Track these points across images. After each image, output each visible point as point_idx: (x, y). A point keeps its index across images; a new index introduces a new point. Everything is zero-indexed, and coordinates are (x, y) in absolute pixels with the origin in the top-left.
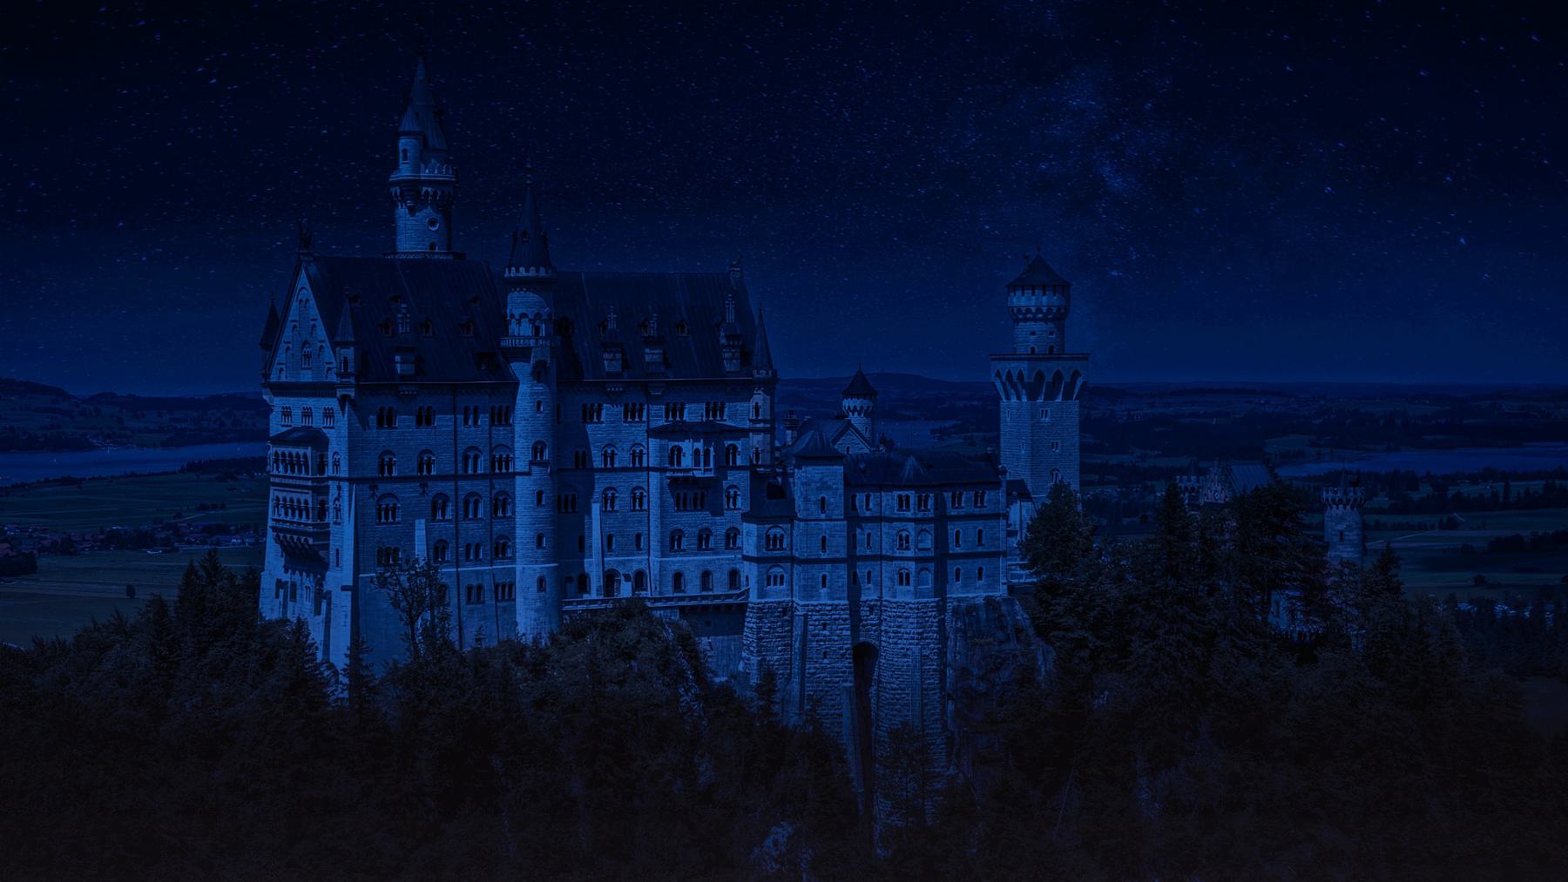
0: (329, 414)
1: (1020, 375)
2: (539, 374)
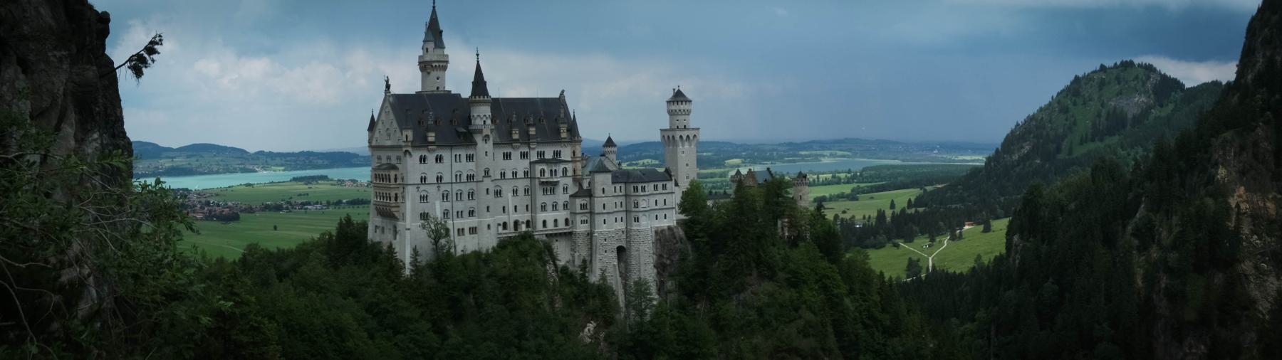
0: (399, 158)
2: (486, 138)
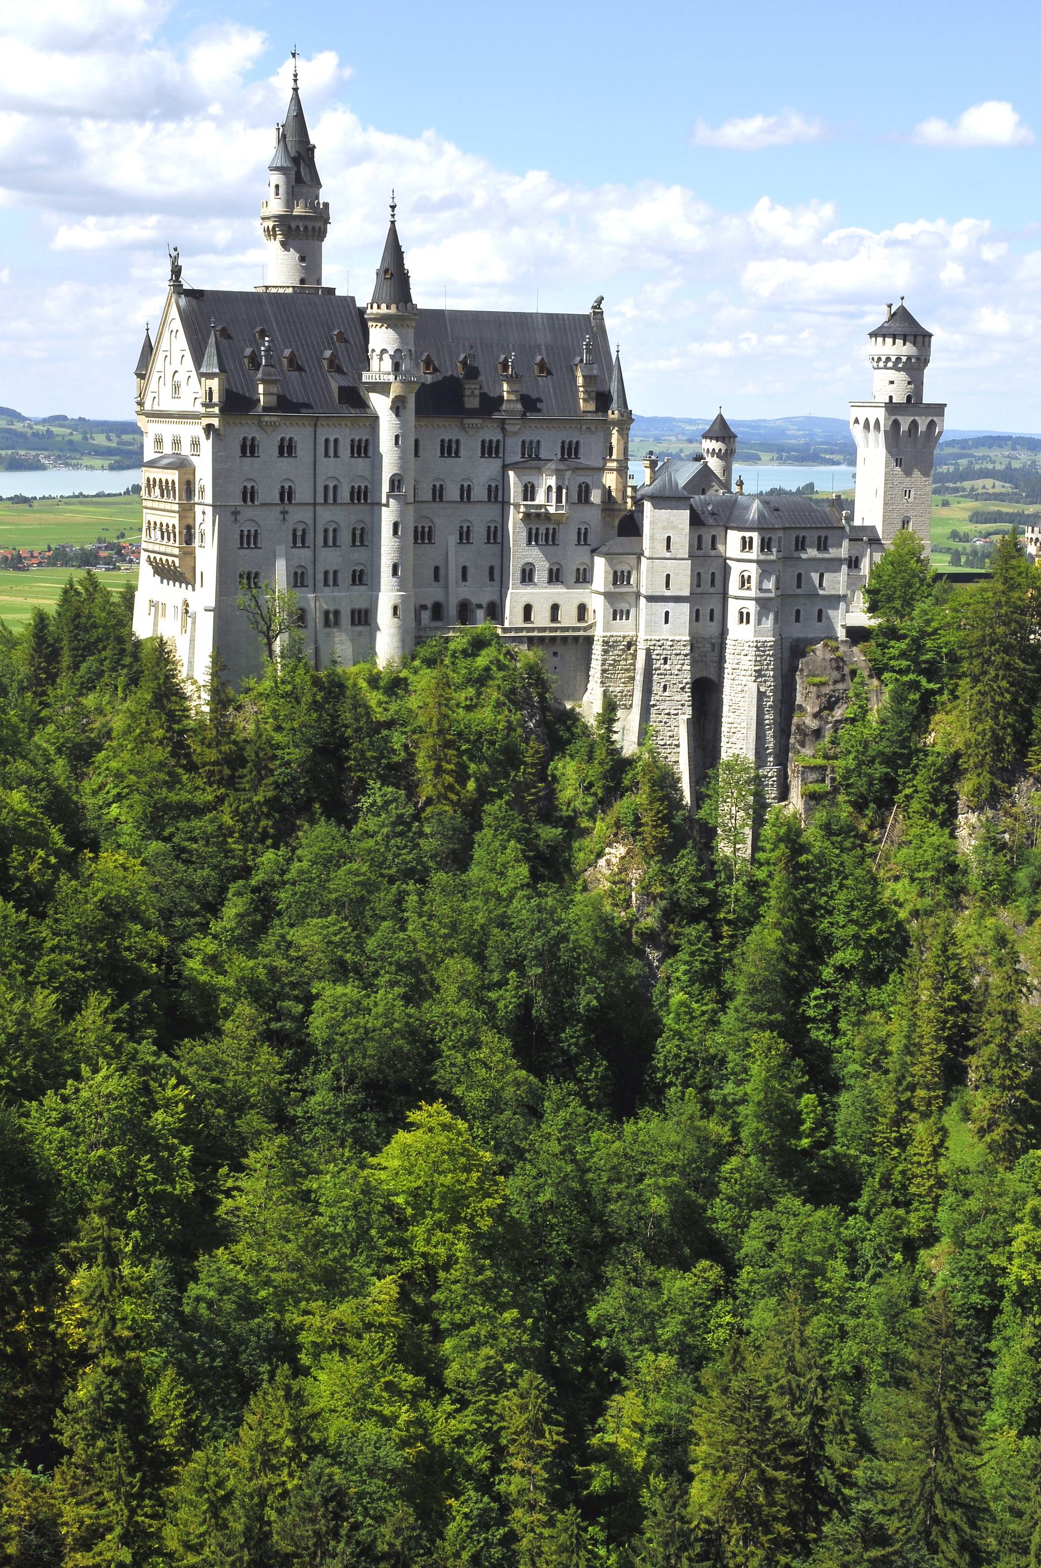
0: (195, 444)
1: (877, 422)
2: (397, 407)
